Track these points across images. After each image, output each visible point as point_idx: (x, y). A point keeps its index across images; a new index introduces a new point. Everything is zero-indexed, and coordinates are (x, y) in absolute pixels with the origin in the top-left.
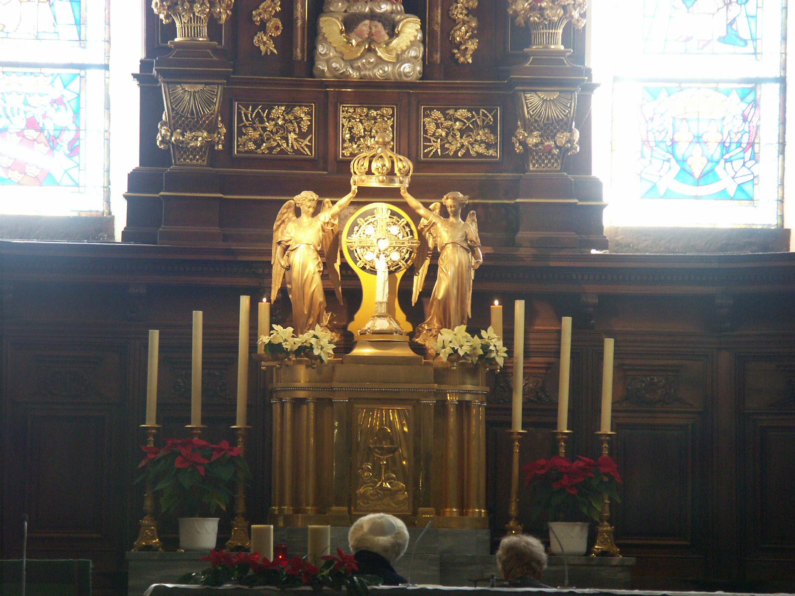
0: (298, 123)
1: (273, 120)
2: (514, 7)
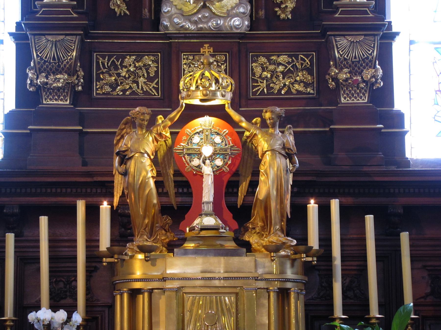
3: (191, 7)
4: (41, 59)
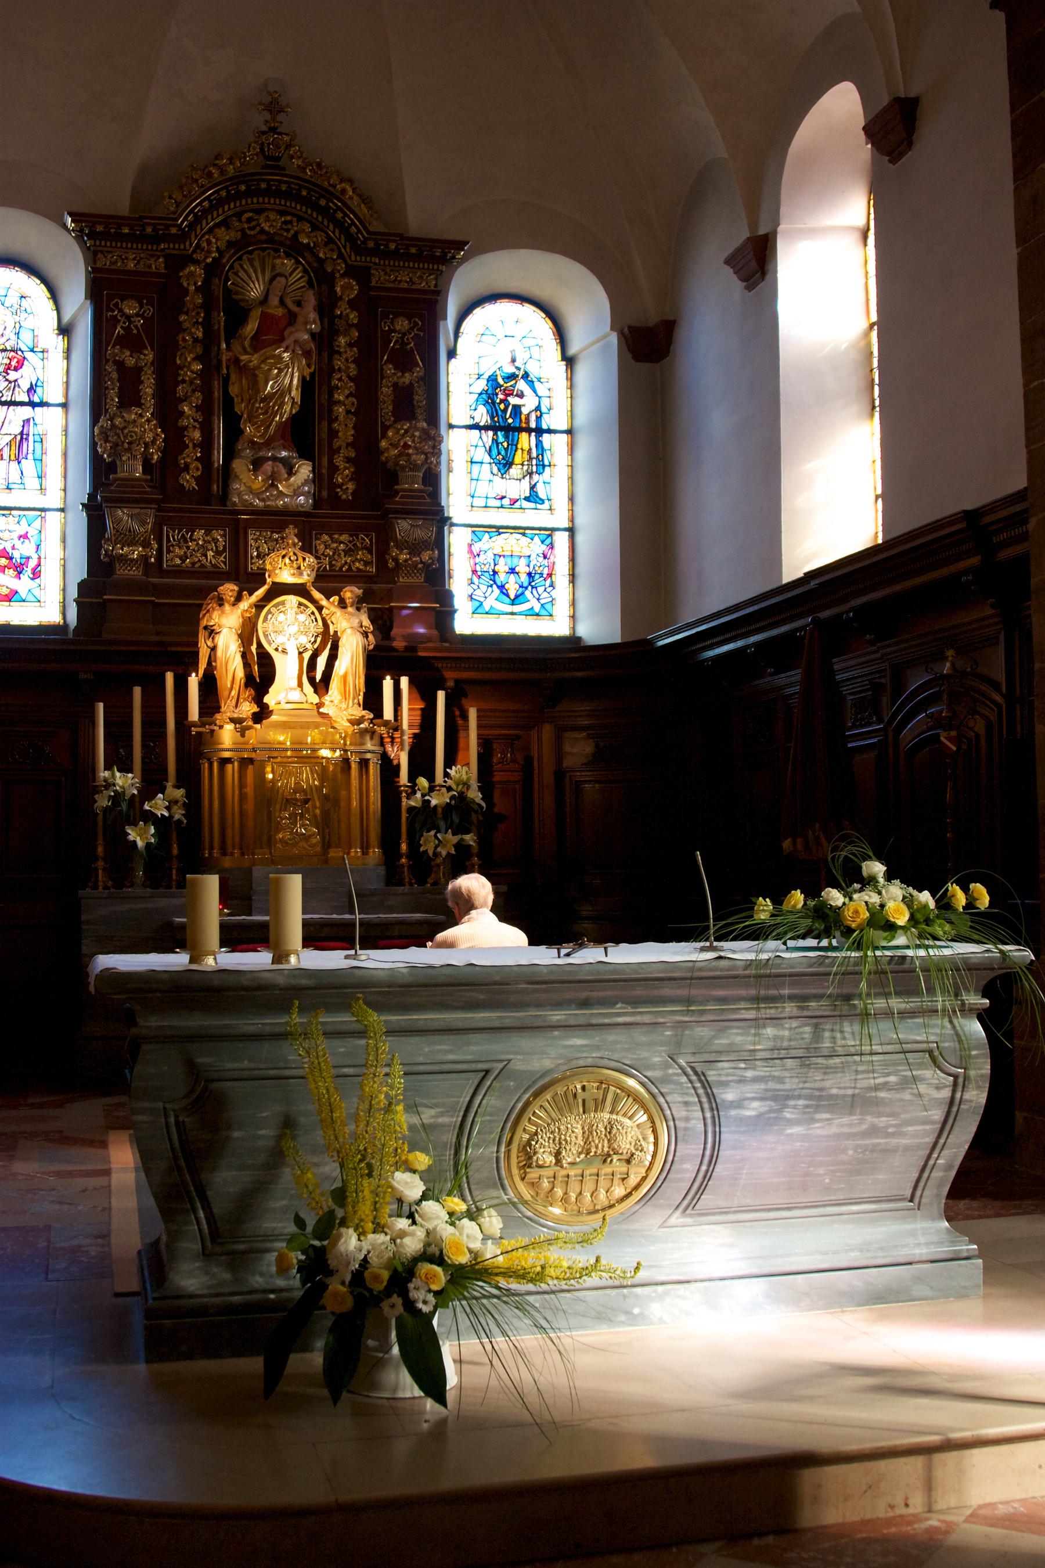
0: (215, 543)
1: (195, 540)
2: (386, 455)
3: (259, 486)
4: (118, 531)
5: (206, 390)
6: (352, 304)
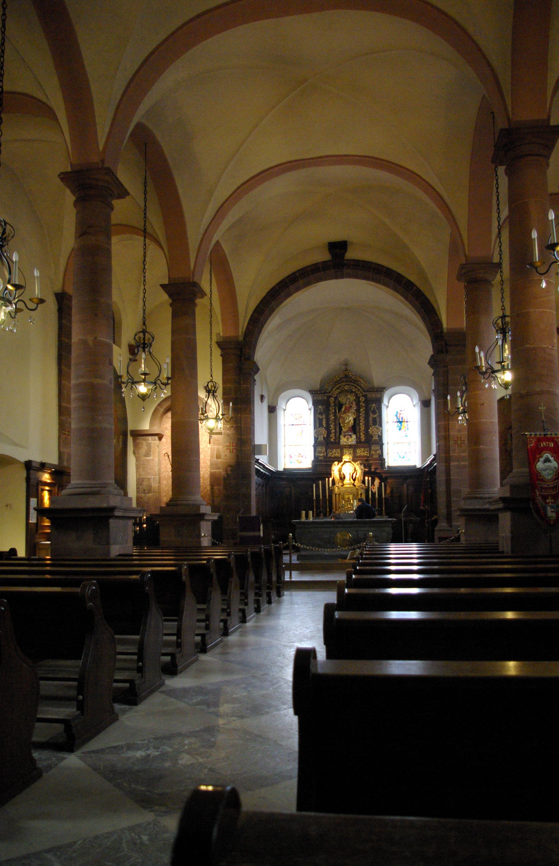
5: (335, 422)
6: (364, 402)
